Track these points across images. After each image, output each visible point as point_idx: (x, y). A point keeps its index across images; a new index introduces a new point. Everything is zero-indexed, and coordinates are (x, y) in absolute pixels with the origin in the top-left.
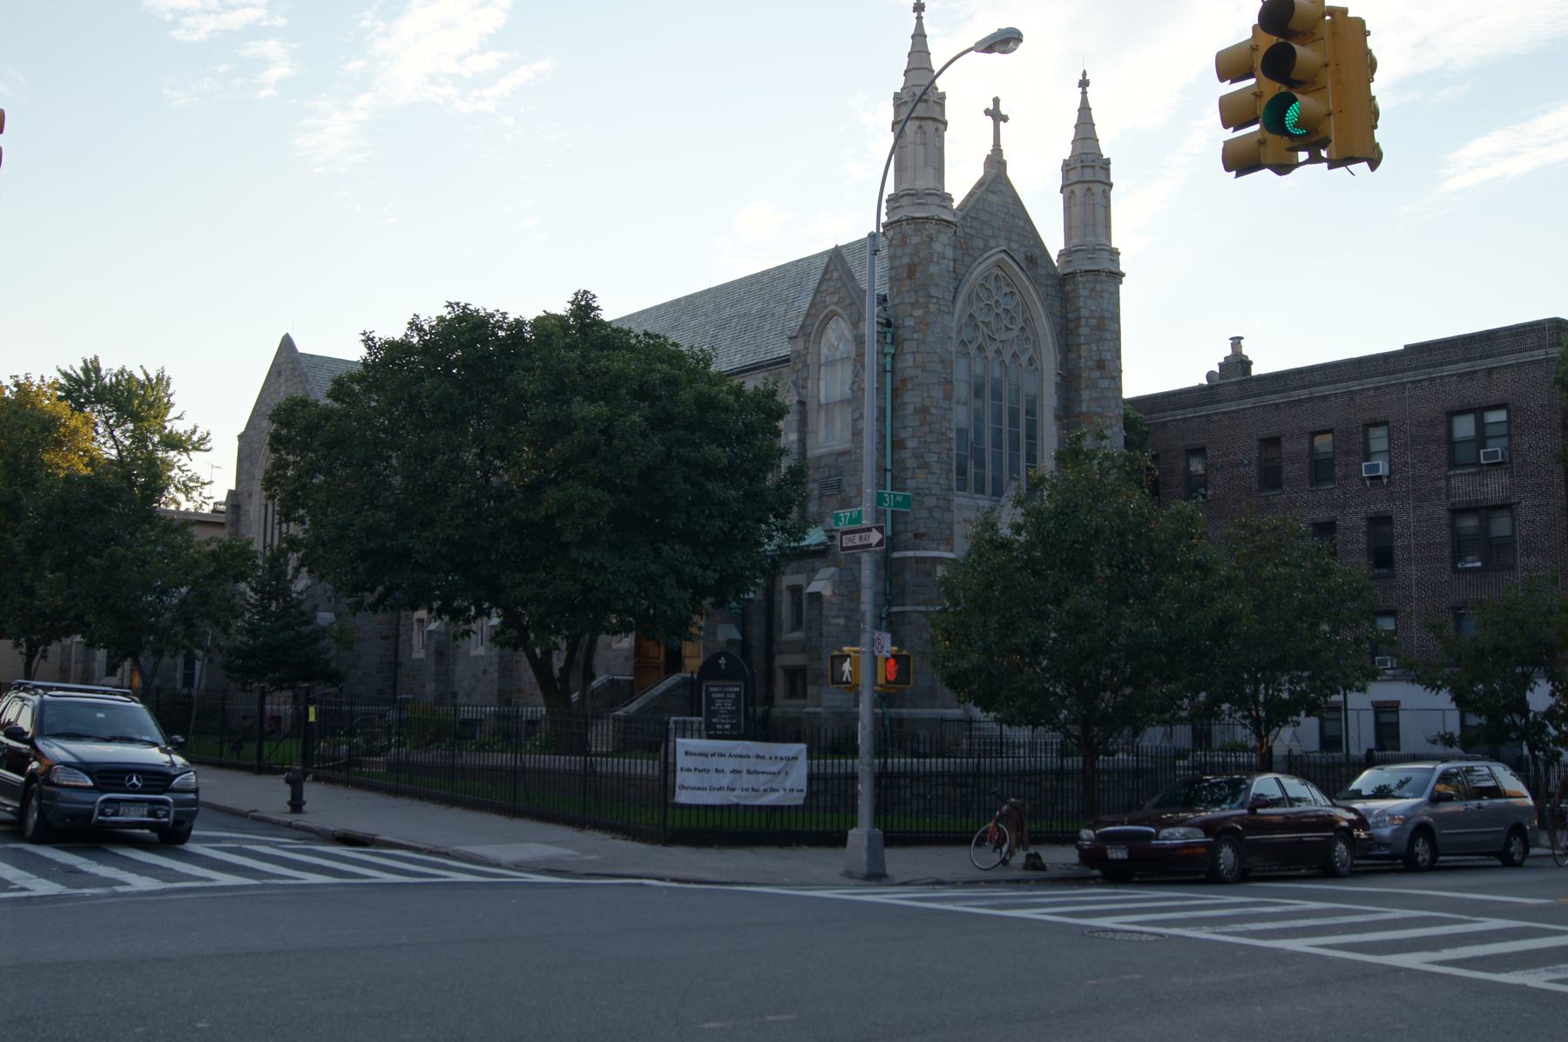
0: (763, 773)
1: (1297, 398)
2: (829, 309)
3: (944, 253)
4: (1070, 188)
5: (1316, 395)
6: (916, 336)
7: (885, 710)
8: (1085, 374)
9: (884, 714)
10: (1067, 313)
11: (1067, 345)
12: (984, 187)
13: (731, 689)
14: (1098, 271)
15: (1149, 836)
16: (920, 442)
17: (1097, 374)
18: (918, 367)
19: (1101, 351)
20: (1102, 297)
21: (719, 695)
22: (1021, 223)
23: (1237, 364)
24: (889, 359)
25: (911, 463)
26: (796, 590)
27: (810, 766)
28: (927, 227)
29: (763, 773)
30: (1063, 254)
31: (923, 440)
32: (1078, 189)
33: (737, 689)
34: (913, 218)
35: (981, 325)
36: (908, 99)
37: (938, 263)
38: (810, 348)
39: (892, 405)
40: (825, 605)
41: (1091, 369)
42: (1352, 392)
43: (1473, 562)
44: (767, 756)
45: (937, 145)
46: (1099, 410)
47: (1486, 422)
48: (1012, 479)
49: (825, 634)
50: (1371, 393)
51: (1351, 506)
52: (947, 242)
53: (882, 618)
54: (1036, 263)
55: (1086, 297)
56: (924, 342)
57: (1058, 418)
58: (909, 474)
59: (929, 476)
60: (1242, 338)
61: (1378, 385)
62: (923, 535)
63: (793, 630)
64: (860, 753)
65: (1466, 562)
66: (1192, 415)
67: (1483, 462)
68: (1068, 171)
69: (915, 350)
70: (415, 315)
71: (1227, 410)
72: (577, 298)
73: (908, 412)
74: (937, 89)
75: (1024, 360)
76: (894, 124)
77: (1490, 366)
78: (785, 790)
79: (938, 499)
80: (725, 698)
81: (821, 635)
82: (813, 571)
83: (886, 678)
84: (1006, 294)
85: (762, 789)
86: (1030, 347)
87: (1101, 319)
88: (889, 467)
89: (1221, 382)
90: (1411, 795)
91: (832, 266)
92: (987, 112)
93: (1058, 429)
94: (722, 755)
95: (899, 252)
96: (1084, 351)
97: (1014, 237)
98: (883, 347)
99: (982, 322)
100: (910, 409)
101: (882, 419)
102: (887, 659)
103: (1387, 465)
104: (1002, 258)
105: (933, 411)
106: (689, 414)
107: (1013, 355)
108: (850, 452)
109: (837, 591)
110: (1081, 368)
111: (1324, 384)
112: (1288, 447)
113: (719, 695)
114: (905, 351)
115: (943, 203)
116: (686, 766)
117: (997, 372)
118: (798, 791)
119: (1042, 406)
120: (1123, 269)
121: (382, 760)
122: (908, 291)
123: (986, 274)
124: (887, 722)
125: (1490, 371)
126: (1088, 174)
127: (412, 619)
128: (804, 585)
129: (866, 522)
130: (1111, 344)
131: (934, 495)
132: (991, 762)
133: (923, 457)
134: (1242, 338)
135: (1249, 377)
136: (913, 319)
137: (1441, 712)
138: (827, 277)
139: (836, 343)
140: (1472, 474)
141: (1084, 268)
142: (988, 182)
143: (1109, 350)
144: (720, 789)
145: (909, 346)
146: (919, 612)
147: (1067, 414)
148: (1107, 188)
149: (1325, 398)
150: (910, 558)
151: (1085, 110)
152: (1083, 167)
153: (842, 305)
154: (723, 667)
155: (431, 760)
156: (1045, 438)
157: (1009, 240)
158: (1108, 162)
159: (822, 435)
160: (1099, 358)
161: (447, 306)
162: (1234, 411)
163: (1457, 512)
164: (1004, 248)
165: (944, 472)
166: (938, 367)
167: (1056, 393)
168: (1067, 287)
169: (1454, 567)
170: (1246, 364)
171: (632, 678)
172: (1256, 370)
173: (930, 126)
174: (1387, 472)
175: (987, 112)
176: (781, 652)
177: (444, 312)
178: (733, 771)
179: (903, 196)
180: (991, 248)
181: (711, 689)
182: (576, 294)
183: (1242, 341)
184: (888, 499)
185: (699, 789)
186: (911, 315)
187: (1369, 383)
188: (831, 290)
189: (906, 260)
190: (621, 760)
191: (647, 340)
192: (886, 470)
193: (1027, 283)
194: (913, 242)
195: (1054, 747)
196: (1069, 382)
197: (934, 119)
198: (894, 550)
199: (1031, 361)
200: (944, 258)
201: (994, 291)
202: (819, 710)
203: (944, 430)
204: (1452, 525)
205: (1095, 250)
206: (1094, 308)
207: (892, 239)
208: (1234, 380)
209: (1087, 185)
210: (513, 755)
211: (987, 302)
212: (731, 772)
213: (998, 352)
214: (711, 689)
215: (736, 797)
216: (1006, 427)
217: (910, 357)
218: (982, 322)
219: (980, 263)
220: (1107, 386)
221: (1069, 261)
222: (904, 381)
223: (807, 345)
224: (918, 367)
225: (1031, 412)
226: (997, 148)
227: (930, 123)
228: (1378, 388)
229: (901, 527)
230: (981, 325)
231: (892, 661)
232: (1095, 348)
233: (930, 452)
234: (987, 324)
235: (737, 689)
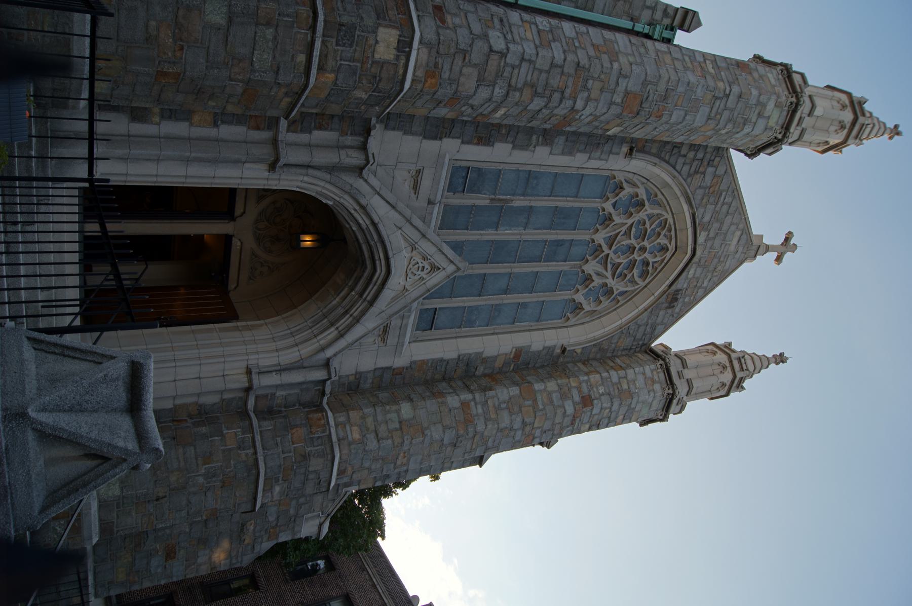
17: (577, 398)
18: (658, 56)
19: (599, 399)
37: (758, 103)
41: (579, 389)
46: (541, 407)
55: (644, 374)
57: (519, 352)
62: (443, 21)
66: (380, 591)
96: (594, 378)
133: (554, 40)
156: (495, 337)
160: (593, 397)
209: (728, 364)
224: (658, 56)
226: (768, 249)
232: (601, 392)
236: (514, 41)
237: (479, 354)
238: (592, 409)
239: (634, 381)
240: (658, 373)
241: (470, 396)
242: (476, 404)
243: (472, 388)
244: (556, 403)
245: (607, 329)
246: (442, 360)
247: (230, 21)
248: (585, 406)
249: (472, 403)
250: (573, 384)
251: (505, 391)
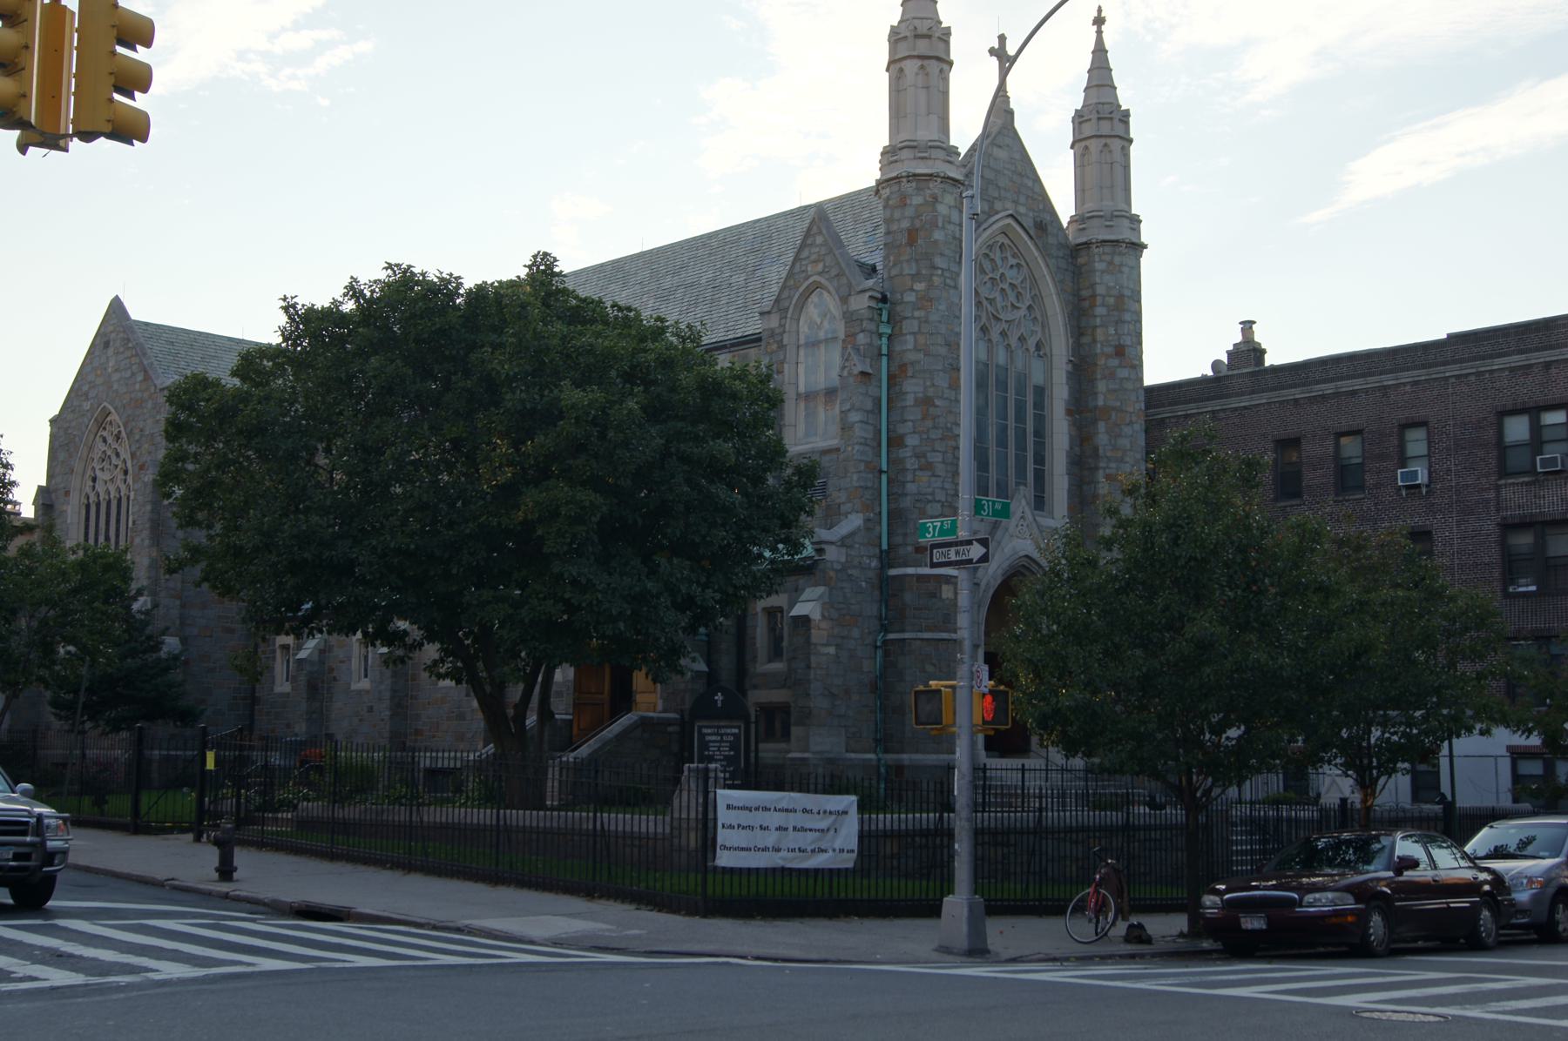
0: (811, 830)
1: (1320, 393)
2: (811, 280)
3: (949, 217)
4: (1083, 144)
5: (1344, 390)
6: (917, 314)
7: (880, 755)
8: (1102, 362)
9: (879, 760)
10: (1079, 290)
11: (1079, 328)
12: (990, 139)
13: (729, 731)
14: (1117, 241)
15: (1291, 903)
16: (921, 439)
17: (1114, 362)
20: (1121, 272)
21: (714, 738)
22: (1030, 184)
23: (1248, 352)
24: (884, 340)
25: (911, 464)
26: (773, 613)
27: (862, 822)
28: (931, 186)
29: (811, 830)
30: (1076, 221)
31: (925, 436)
32: (1094, 145)
33: (736, 731)
34: (915, 175)
35: (985, 303)
36: (908, 34)
37: (943, 228)
38: (787, 326)
39: (888, 394)
40: (813, 631)
42: (1385, 387)
43: (1527, 585)
44: (815, 811)
45: (941, 89)
46: (1119, 404)
47: (1542, 424)
48: (1018, 484)
49: (813, 665)
50: (1408, 388)
51: (1383, 519)
52: (952, 203)
53: (876, 647)
54: (1046, 230)
55: (1103, 272)
56: (926, 321)
57: (1069, 412)
58: (909, 477)
59: (933, 479)
60: (1254, 322)
61: (1416, 379)
63: (770, 661)
64: (958, 807)
65: (1519, 586)
67: (1539, 470)
68: (1080, 123)
69: (916, 329)
70: (352, 277)
71: (1237, 405)
72: (535, 262)
73: (908, 404)
74: (941, 23)
75: (1031, 343)
76: (891, 63)
77: (1548, 359)
78: (834, 850)
79: (943, 506)
80: (721, 741)
81: (809, 667)
82: (796, 590)
83: (983, 718)
84: (1012, 266)
85: (809, 849)
86: (1038, 328)
87: (1120, 297)
88: (884, 467)
89: (1230, 373)
90: (1546, 854)
91: (815, 229)
92: (992, 52)
93: (1069, 425)
94: (766, 809)
95: (897, 214)
97: (1022, 199)
98: (878, 327)
99: (987, 299)
100: (910, 400)
101: (877, 411)
102: (984, 695)
103: (1426, 472)
104: (1009, 224)
105: (937, 402)
106: (691, 403)
107: (1019, 339)
108: (838, 450)
109: (826, 614)
110: (1096, 354)
111: (1354, 377)
112: (1311, 449)
113: (714, 738)
114: (904, 332)
115: (949, 158)
116: (728, 822)
117: (1001, 357)
118: (848, 852)
119: (1052, 398)
120: (1144, 239)
121: (290, 816)
122: (908, 261)
123: (990, 243)
124: (883, 770)
125: (1547, 365)
126: (1105, 128)
127: (274, 645)
128: (785, 608)
129: (963, 534)
130: (1131, 327)
131: (939, 501)
132: (1028, 816)
133: (924, 456)
134: (1254, 322)
135: (1262, 368)
136: (914, 294)
137: (1492, 759)
138: (809, 242)
139: (819, 321)
140: (1527, 484)
141: (1101, 237)
142: (993, 135)
143: (1129, 334)
144: (765, 849)
145: (909, 326)
146: (922, 639)
147: (1081, 410)
148: (1126, 144)
149: (1354, 393)
150: (912, 575)
151: (1100, 52)
152: (1099, 119)
153: (827, 277)
154: (719, 704)
155: (357, 816)
157: (1016, 202)
158: (1127, 114)
159: (801, 427)
161: (386, 268)
162: (1245, 408)
163: (1509, 527)
164: (1010, 212)
165: (950, 475)
166: (943, 351)
167: (1067, 384)
168: (1079, 260)
169: (1505, 590)
170: (1259, 353)
171: (570, 717)
172: (1269, 360)
173: (933, 66)
174: (1426, 480)
175: (992, 52)
176: (755, 687)
177: (383, 275)
178: (779, 829)
179: (901, 149)
180: (997, 213)
181: (705, 731)
182: (535, 257)
183: (1254, 326)
184: (986, 507)
185: (743, 849)
186: (912, 289)
187: (1406, 377)
188: (813, 257)
189: (905, 224)
190: (613, 815)
191: (616, 313)
192: (881, 472)
193: (1036, 254)
194: (914, 202)
195: (1091, 799)
196: (1082, 371)
197: (938, 59)
198: (891, 566)
199: (1038, 346)
200: (950, 222)
201: (999, 262)
202: (806, 755)
203: (949, 425)
204: (1503, 544)
205: (1113, 217)
206: (1112, 284)
207: (888, 199)
208: (1245, 371)
209: (1103, 141)
210: (494, 811)
211: (991, 275)
212: (777, 829)
213: (1003, 334)
214: (705, 731)
215: (781, 858)
216: (1011, 423)
217: (910, 338)
218: (987, 299)
219: (985, 229)
220: (1127, 376)
221: (1084, 229)
222: (903, 367)
223: (783, 321)
225: (1039, 405)
227: (933, 62)
228: (1416, 383)
229: (898, 539)
230: (985, 303)
231: (989, 698)
233: (934, 451)
234: (991, 301)
235: (736, 731)
236: (933, 494)
237: (1069, 454)
238: (1128, 346)
239: (1109, 288)
240: (1104, 253)
241: (1101, 472)
242: (1108, 467)
243: (1093, 466)
244: (1117, 387)
245: (1058, 310)
246: (1069, 491)
248: (1124, 355)
249: (1108, 471)
250: (1103, 362)
251: (1100, 436)
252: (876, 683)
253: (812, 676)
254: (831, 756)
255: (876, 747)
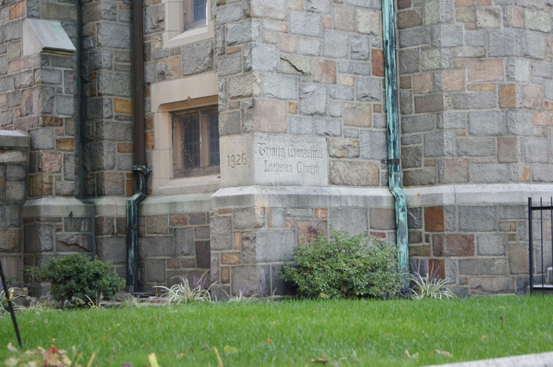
7: (397, 190)
124: (402, 217)
176: (162, 76)
247: (526, 56)
252: (384, 53)
253: (255, 34)
254: (300, 191)
255: (389, 174)
